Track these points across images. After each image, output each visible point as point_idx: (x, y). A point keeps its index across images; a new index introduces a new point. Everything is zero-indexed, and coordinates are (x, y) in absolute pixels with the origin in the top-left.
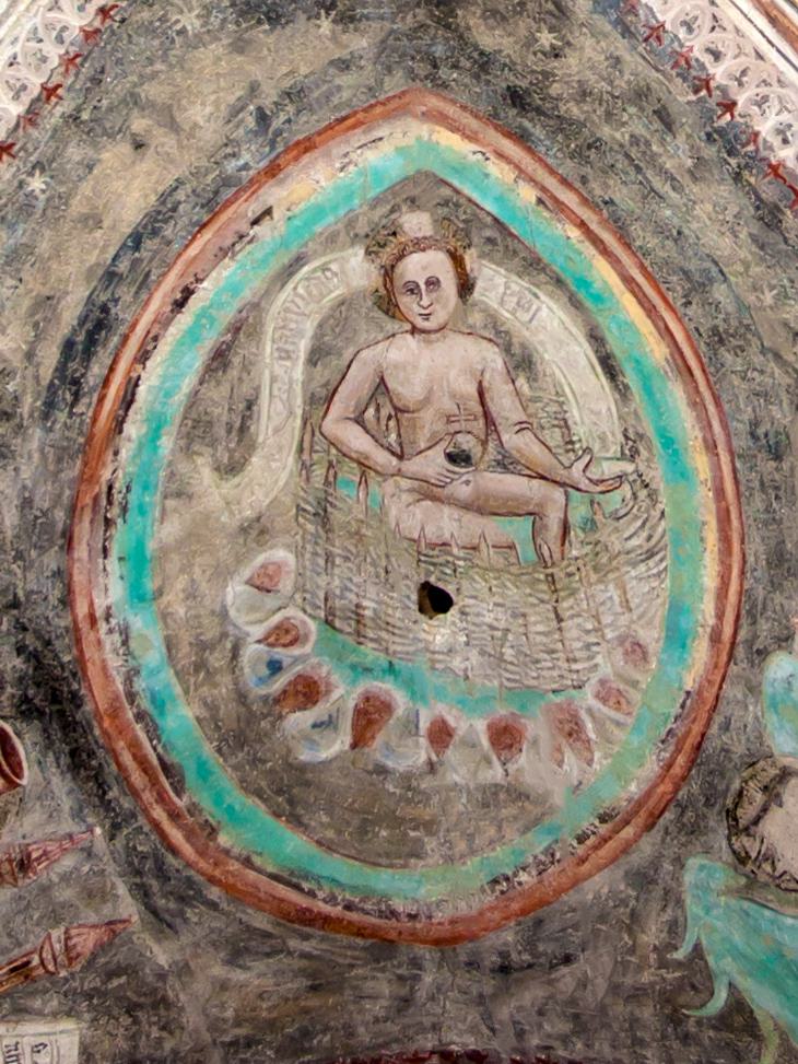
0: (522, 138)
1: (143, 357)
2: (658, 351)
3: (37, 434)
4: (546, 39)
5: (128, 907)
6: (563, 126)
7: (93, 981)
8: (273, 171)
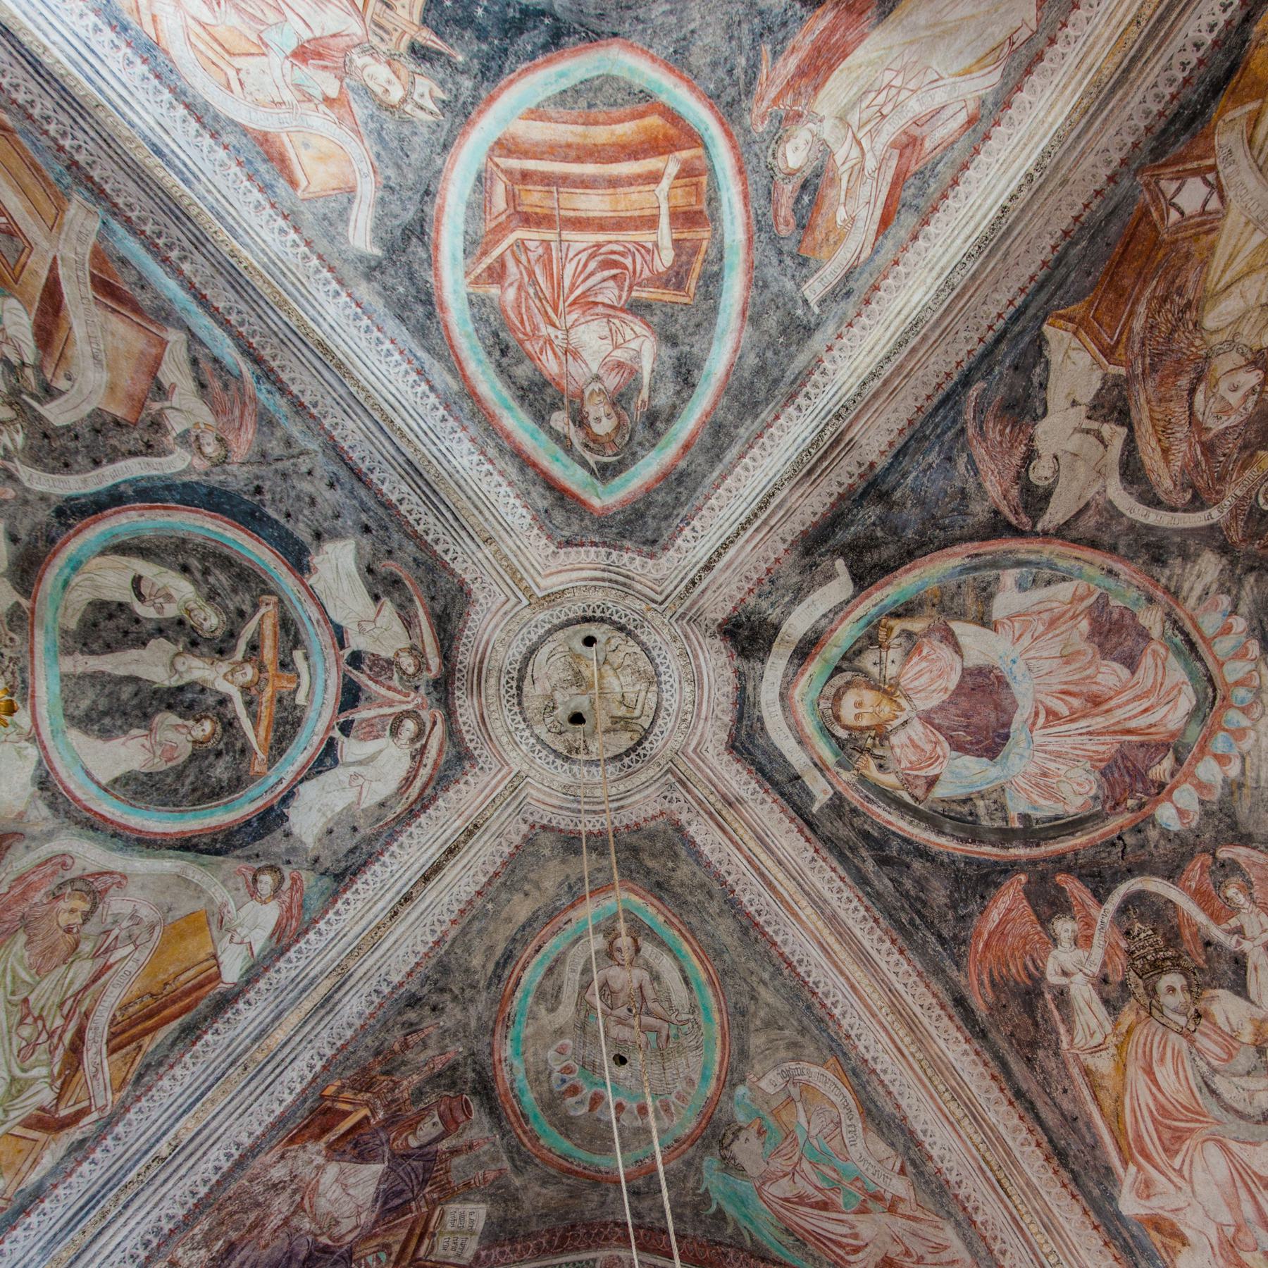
0: (660, 899)
1: (524, 969)
2: (703, 976)
3: (485, 994)
4: (670, 865)
5: (507, 1164)
6: (675, 896)
7: (492, 1191)
8: (573, 906)
